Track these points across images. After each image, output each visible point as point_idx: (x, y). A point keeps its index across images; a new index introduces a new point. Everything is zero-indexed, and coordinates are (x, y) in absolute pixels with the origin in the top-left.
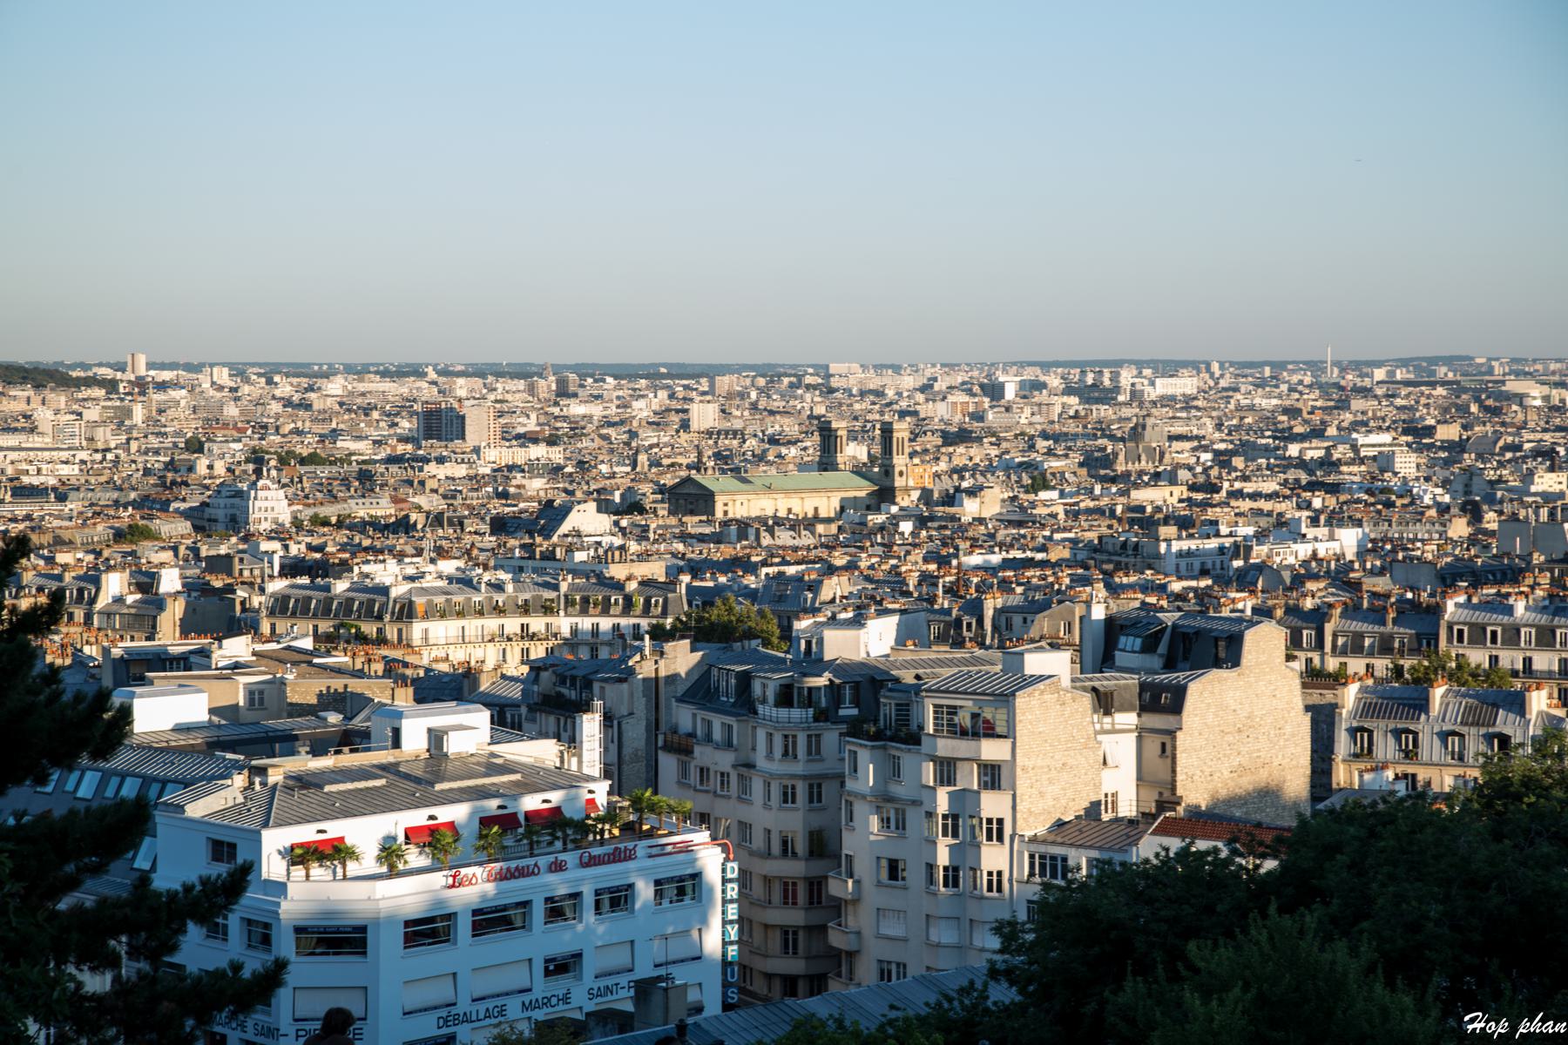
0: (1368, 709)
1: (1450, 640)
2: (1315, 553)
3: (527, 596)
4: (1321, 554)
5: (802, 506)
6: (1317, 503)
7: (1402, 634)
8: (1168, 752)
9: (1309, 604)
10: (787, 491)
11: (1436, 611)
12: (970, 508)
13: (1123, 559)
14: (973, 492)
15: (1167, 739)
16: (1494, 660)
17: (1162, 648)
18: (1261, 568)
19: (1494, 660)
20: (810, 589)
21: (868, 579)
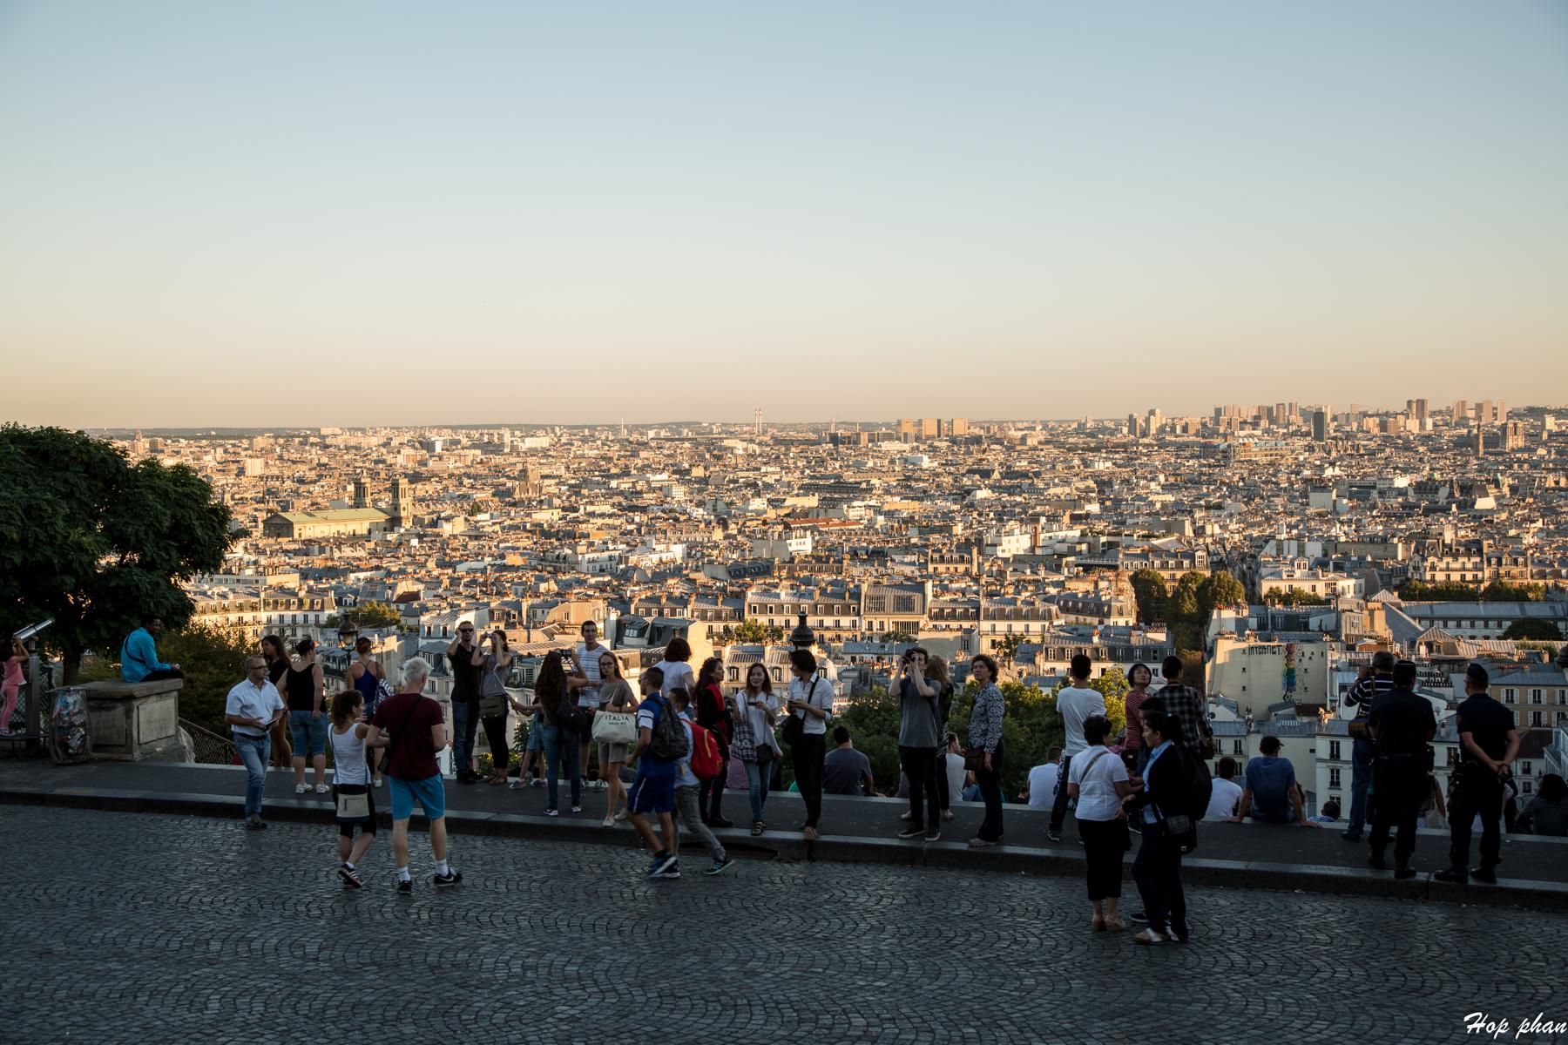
0: (736, 658)
1: (750, 612)
2: (661, 559)
3: (242, 601)
4: (664, 560)
5: (347, 528)
6: (637, 519)
7: (726, 609)
9: (677, 593)
10: (336, 521)
11: (739, 596)
12: (447, 529)
13: (558, 565)
14: (448, 519)
16: (771, 621)
17: (647, 635)
18: (635, 568)
19: (771, 621)
20: (390, 588)
21: (418, 579)
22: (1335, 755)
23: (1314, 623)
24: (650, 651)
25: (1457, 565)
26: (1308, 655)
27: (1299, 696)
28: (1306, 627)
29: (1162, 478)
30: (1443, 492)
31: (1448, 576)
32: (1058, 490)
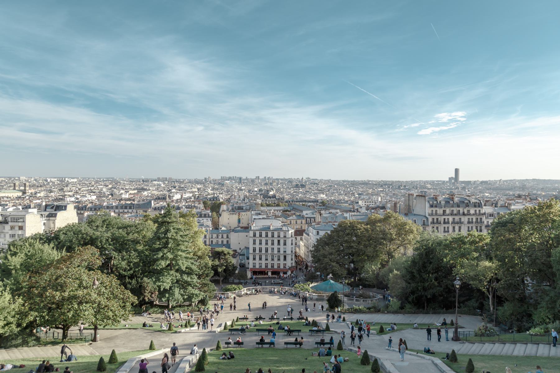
4: (89, 199)
5: (10, 195)
8: (54, 223)
10: (7, 193)
12: (38, 195)
14: (39, 193)
15: (54, 221)
17: (54, 208)
22: (255, 235)
23: (244, 208)
24: (53, 212)
25: (271, 200)
26: (243, 215)
27: (241, 225)
28: (243, 209)
29: (211, 188)
30: (264, 191)
31: (269, 202)
32: (189, 190)
